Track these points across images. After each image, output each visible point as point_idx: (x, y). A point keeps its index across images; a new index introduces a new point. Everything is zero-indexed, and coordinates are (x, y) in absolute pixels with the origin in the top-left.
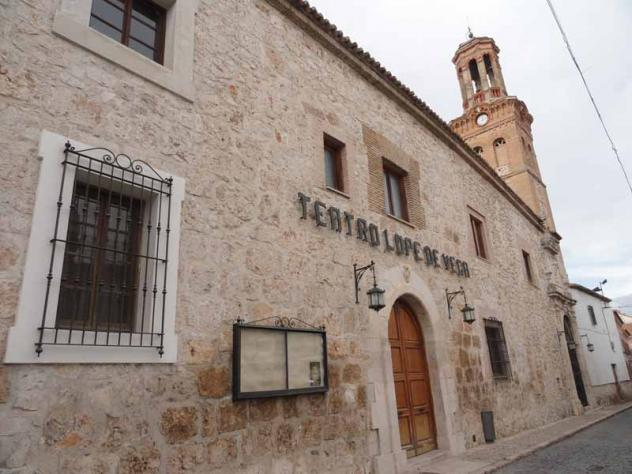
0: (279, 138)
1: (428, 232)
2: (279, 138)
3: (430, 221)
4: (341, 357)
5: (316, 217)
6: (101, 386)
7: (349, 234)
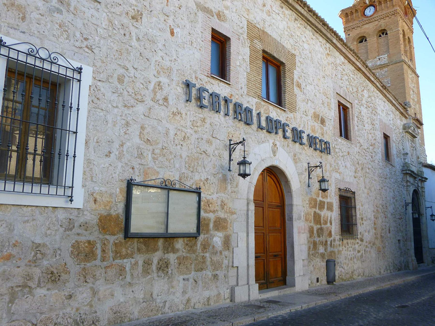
0: (172, 33)
1: (298, 115)
2: (172, 33)
3: (301, 105)
4: (214, 212)
5: (199, 99)
6: (27, 221)
7: (227, 115)
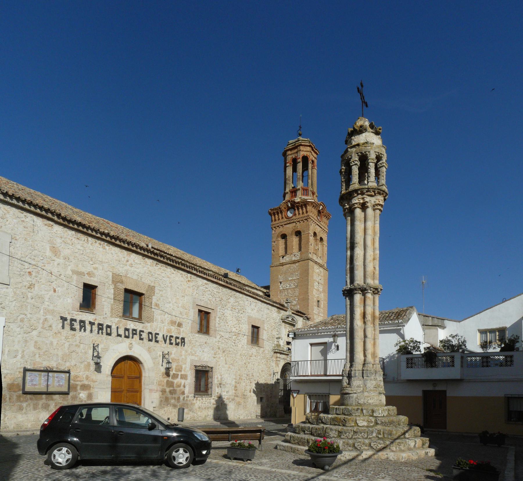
0: (55, 291)
2: (55, 291)
4: (81, 381)
